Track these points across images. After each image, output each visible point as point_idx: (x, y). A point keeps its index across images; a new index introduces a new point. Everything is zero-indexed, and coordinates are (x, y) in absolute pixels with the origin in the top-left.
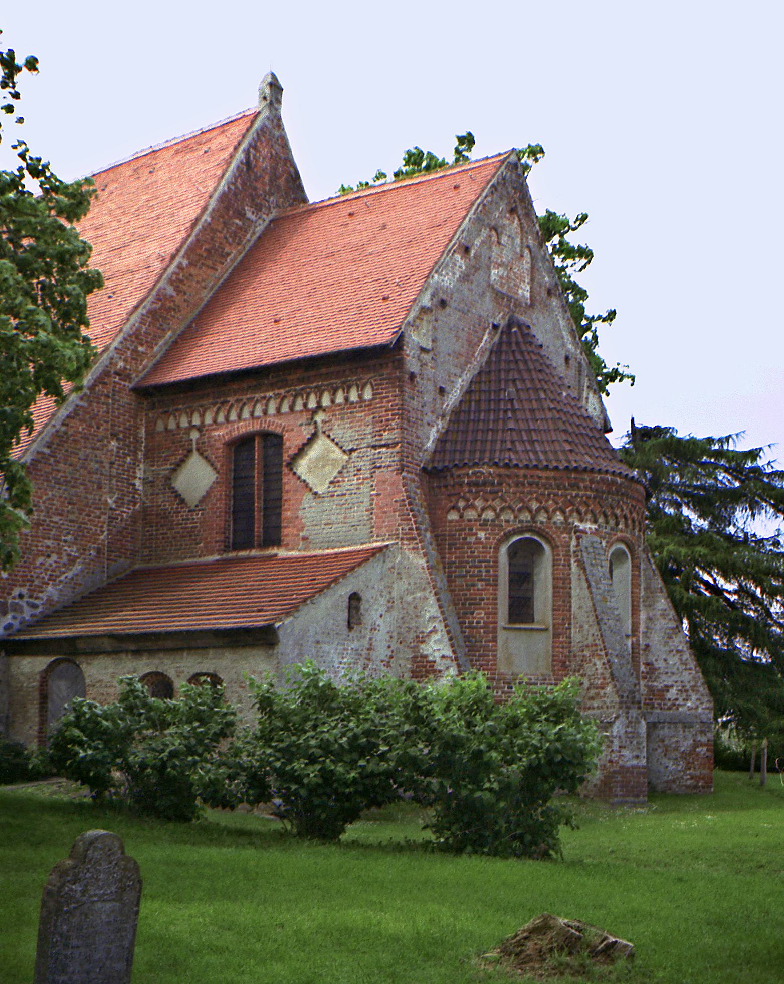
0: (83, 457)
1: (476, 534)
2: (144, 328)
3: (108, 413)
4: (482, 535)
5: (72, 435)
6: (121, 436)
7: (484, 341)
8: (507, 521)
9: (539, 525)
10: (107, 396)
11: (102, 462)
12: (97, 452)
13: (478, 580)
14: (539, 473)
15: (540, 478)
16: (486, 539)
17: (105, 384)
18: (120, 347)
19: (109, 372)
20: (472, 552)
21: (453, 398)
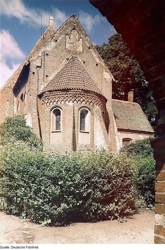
2: (15, 77)
7: (63, 63)
12: (4, 104)
14: (58, 92)
21: (50, 78)
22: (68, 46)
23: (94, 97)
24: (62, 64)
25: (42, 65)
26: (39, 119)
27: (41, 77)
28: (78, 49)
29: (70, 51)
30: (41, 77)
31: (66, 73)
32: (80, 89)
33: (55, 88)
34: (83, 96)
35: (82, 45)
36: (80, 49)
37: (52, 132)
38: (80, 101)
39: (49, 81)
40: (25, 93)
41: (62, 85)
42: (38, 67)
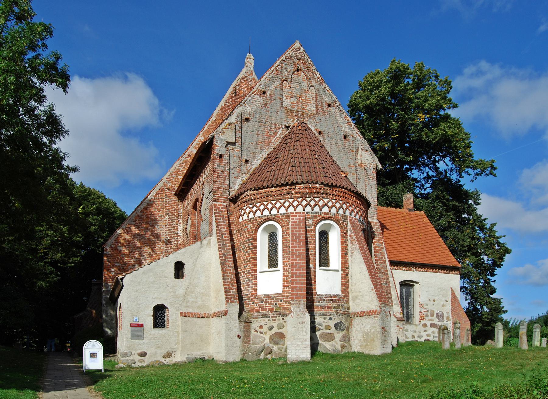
0: (151, 224)
1: (247, 226)
3: (164, 205)
4: (249, 226)
5: (146, 216)
6: (170, 214)
8: (259, 217)
9: (273, 216)
10: (164, 199)
11: (161, 225)
13: (249, 249)
14: (271, 189)
15: (272, 192)
16: (251, 228)
17: (162, 193)
18: (169, 177)
19: (164, 188)
20: (246, 236)
21: (254, 165)
22: (286, 102)
23: (346, 198)
24: (276, 137)
25: (238, 140)
26: (233, 247)
27: (235, 164)
28: (308, 108)
29: (292, 111)
30: (235, 164)
31: (286, 153)
32: (317, 183)
33: (265, 183)
34: (324, 195)
35: (314, 100)
36: (312, 107)
37: (260, 272)
38: (328, 206)
39: (251, 171)
40: (203, 197)
41: (280, 176)
42: (229, 143)
